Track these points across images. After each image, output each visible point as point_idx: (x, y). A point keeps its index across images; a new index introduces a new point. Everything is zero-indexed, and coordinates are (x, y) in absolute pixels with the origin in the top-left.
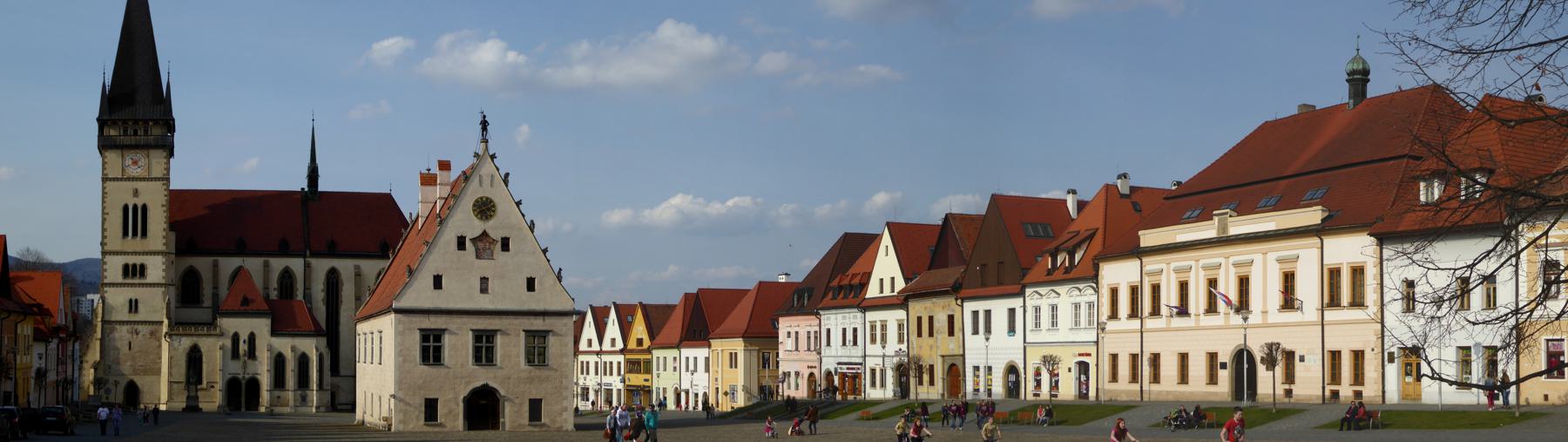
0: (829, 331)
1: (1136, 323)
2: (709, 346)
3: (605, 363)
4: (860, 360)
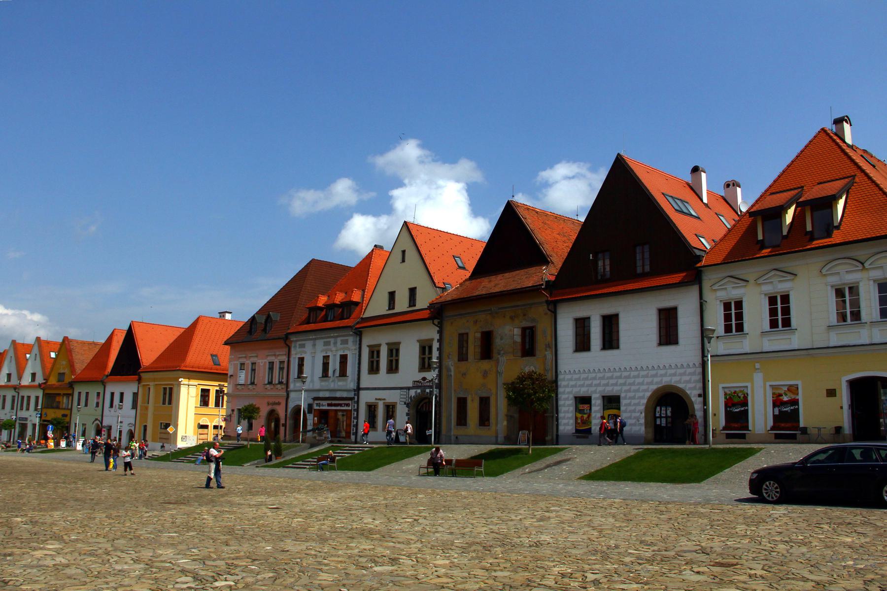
0: (301, 360)
2: (139, 380)
3: (23, 397)
4: (351, 395)
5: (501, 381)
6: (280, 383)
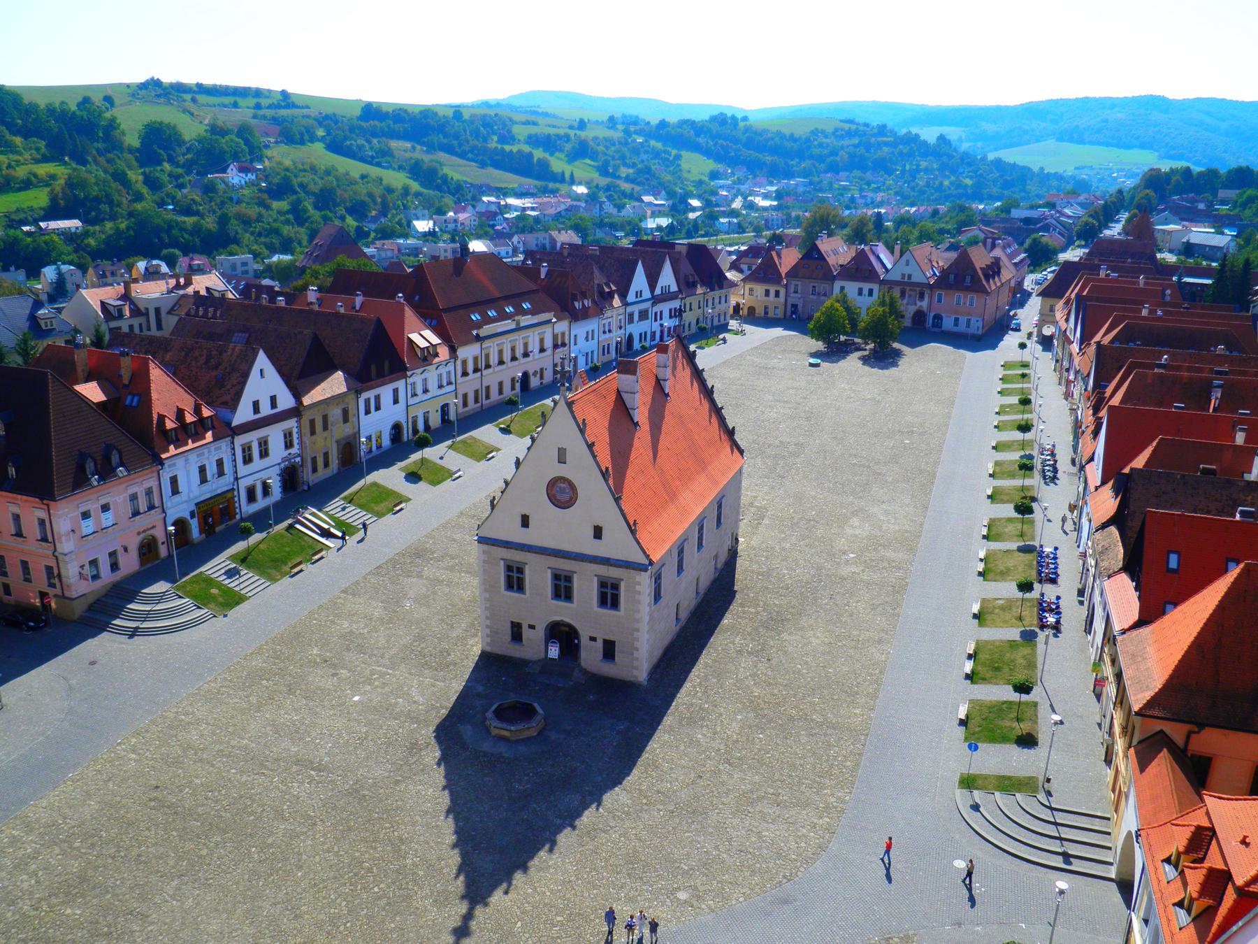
1: (479, 374)
4: (231, 487)
5: (334, 440)
6: (151, 507)
